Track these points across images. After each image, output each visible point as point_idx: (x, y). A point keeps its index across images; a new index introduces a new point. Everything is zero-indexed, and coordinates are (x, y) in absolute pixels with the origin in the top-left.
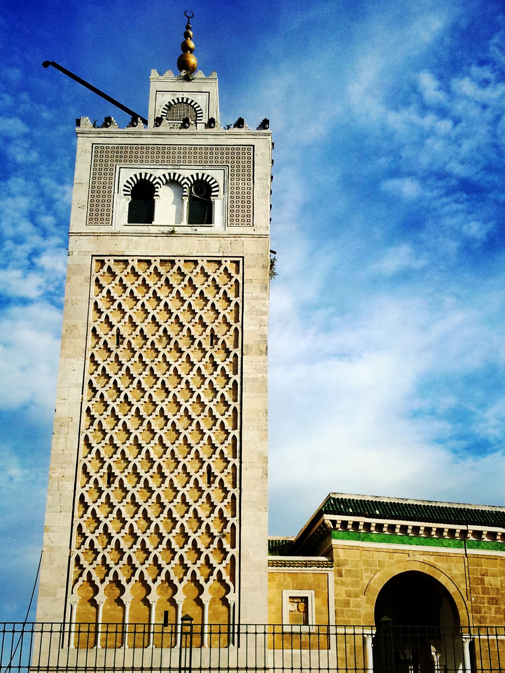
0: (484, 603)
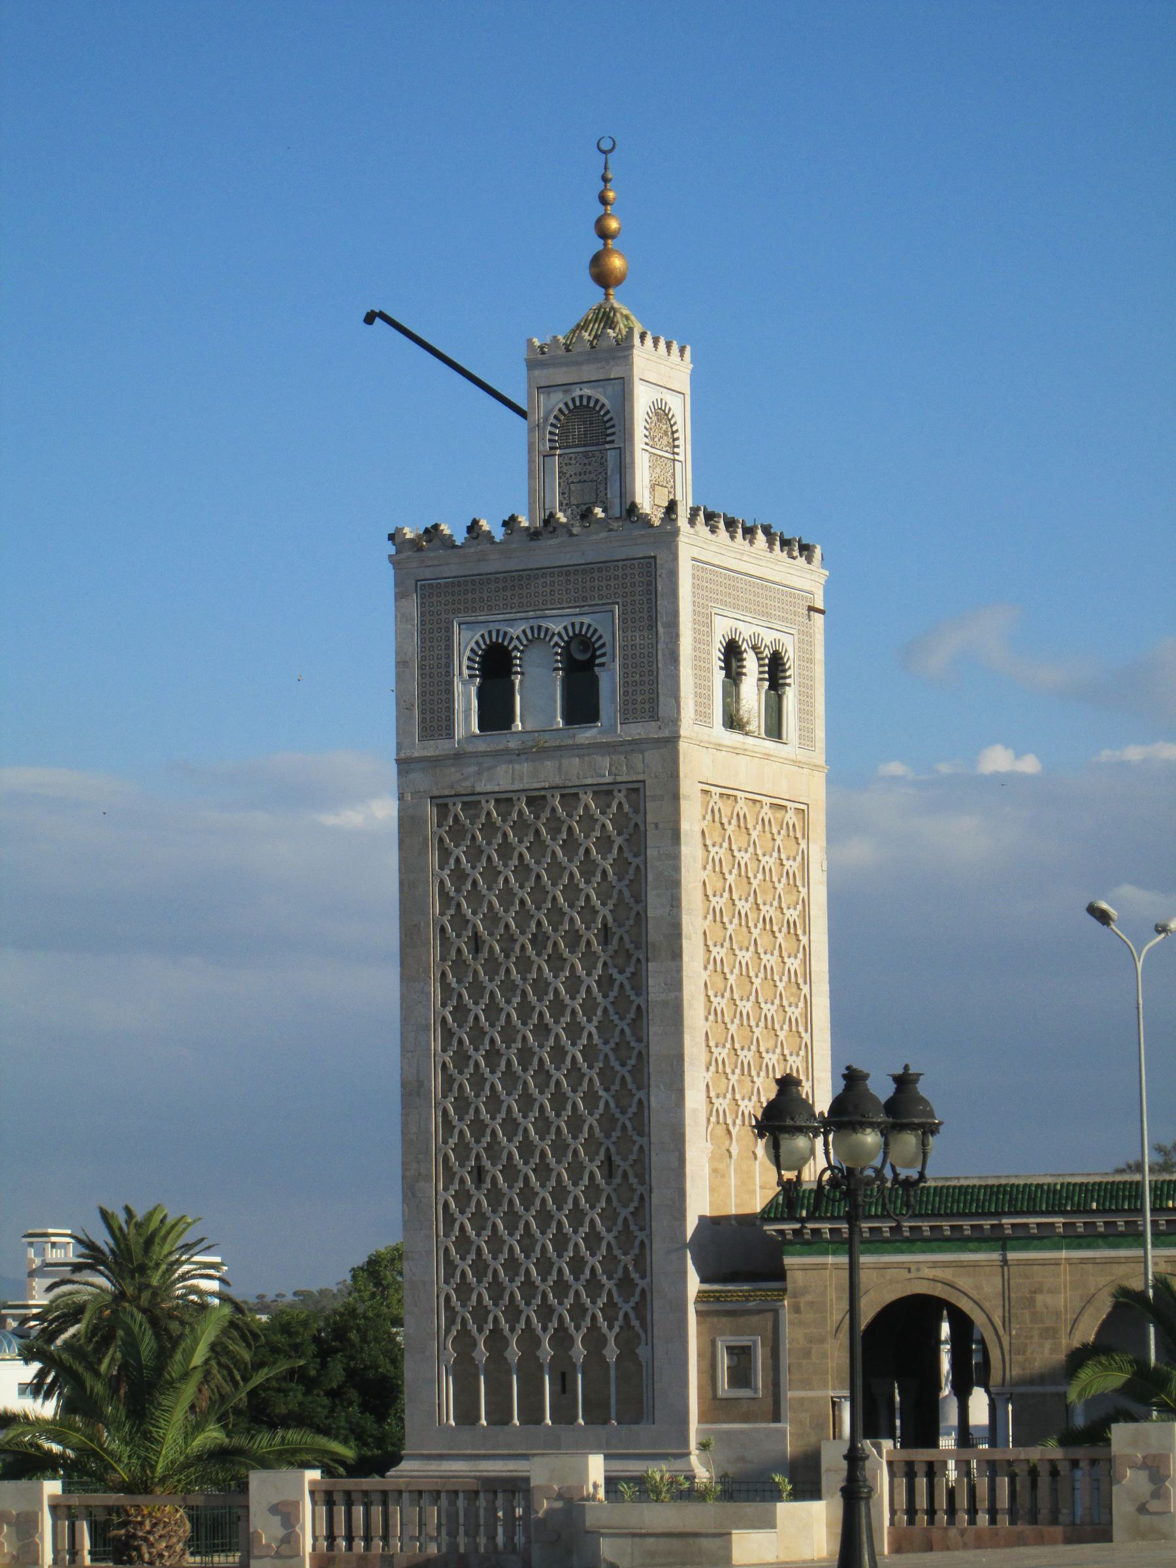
0: (1032, 1337)
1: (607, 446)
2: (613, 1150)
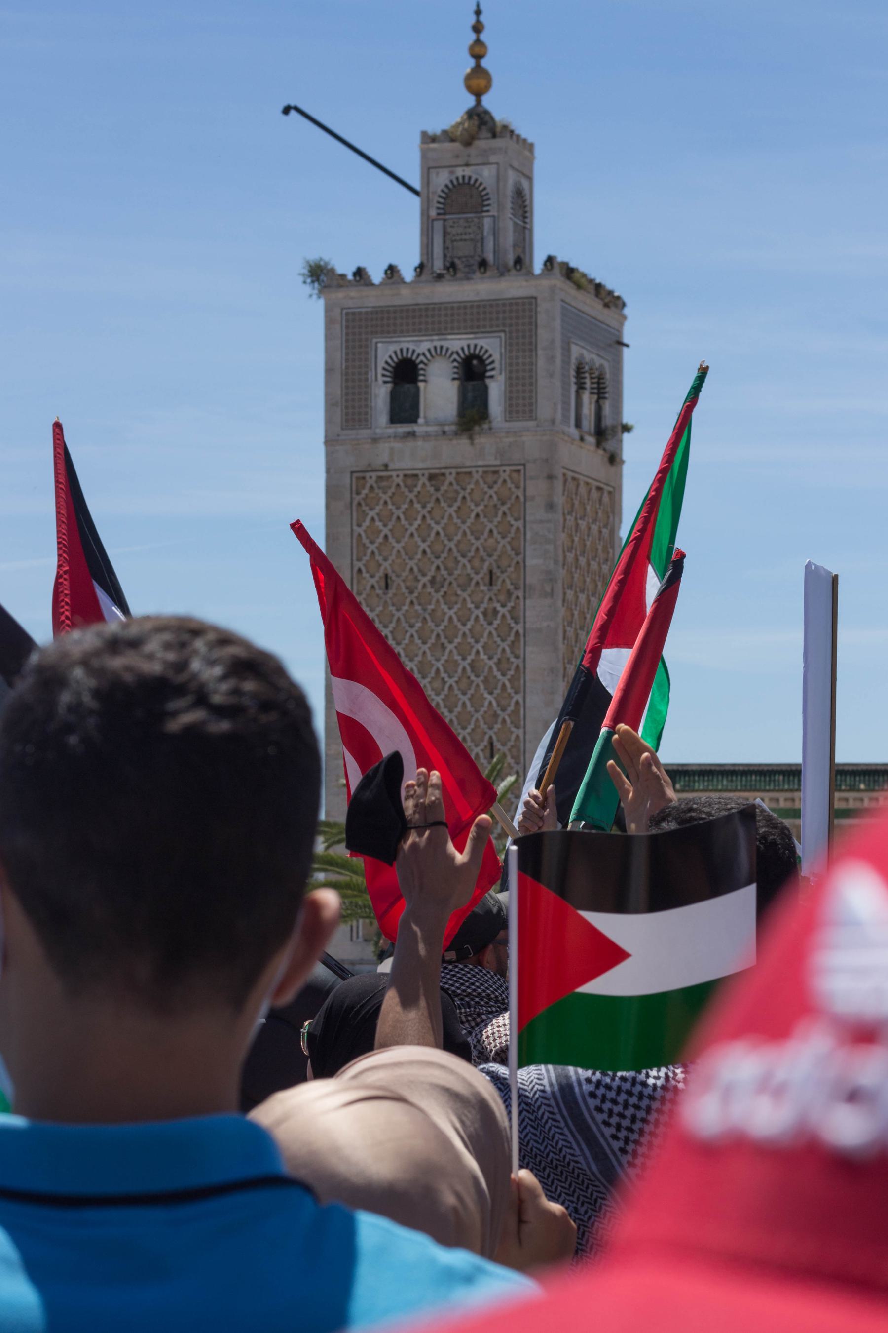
1: (484, 214)
2: (495, 738)
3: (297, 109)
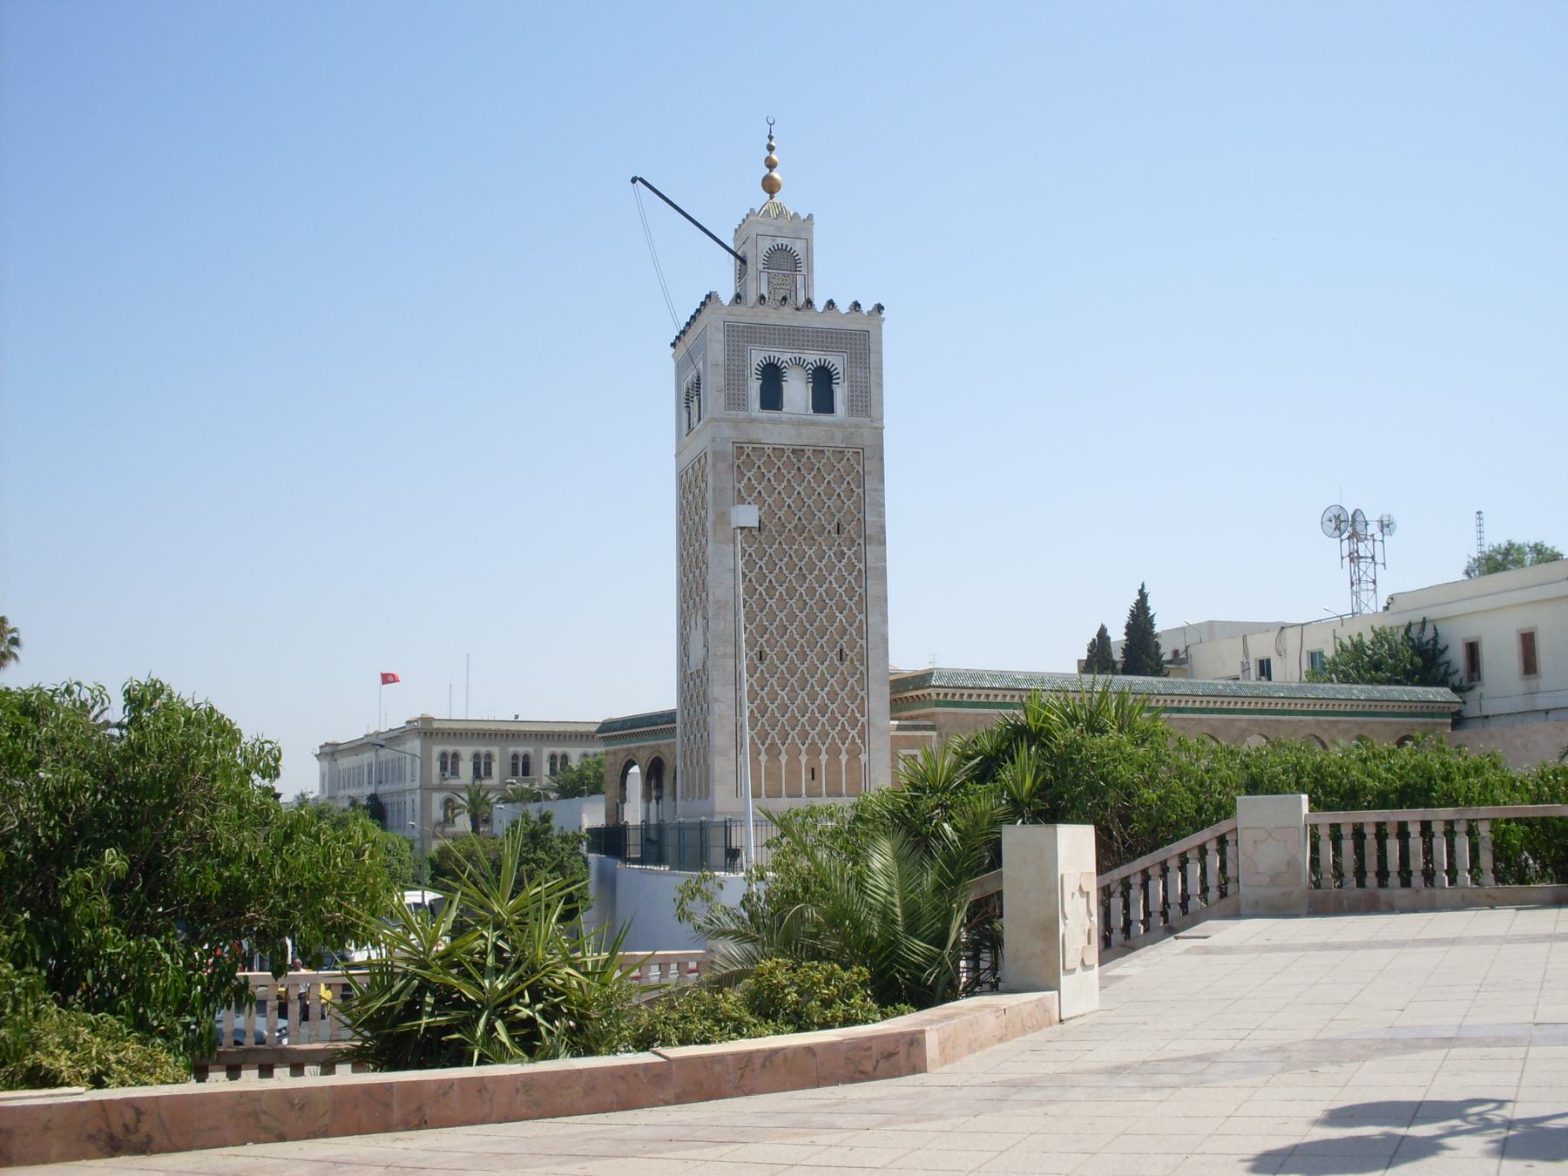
3: (642, 180)
